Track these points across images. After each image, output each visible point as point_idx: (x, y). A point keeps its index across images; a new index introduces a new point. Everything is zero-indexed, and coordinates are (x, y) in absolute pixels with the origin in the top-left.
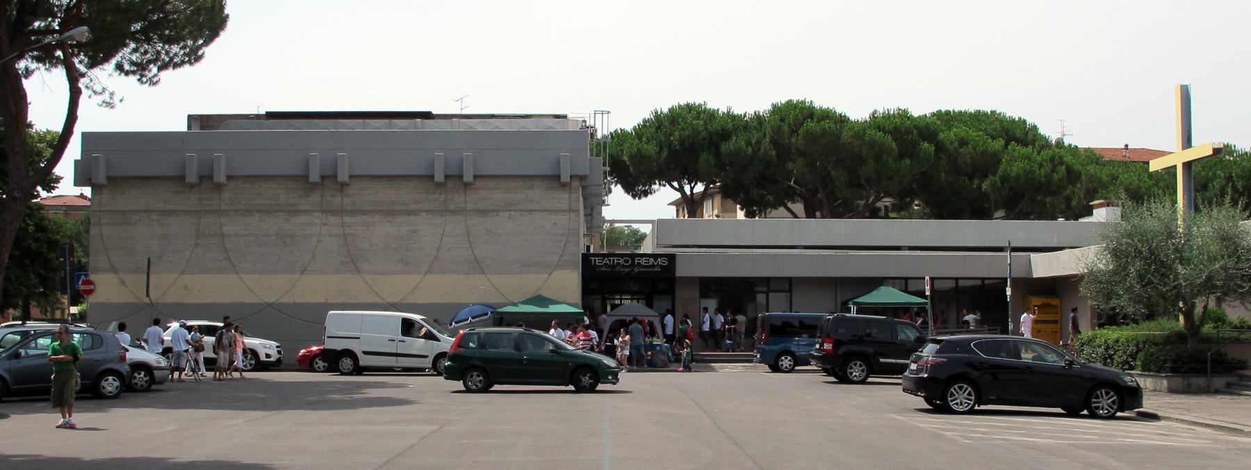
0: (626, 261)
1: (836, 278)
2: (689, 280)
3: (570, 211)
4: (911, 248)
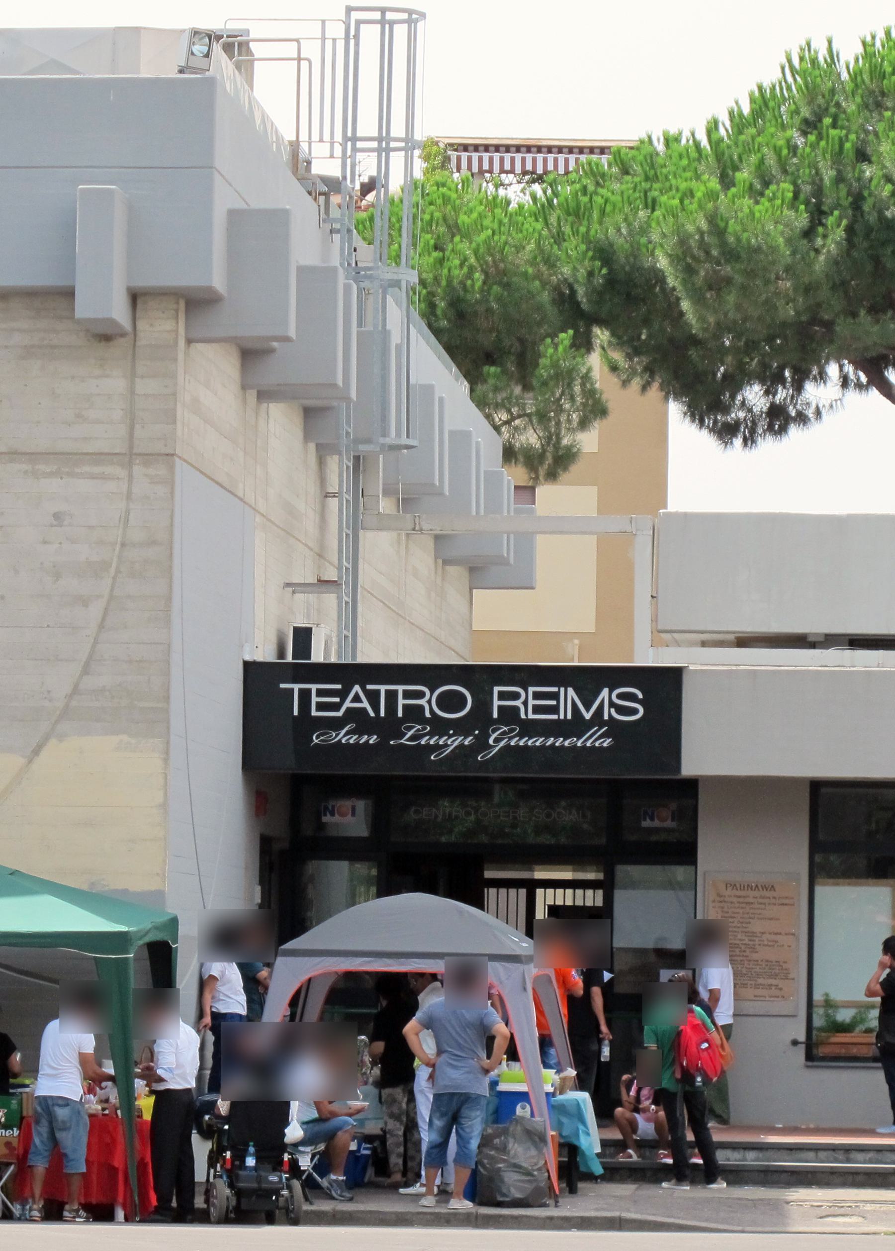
0: (450, 702)
1: (635, 949)
2: (755, 795)
3: (130, 457)
4: (830, 641)
